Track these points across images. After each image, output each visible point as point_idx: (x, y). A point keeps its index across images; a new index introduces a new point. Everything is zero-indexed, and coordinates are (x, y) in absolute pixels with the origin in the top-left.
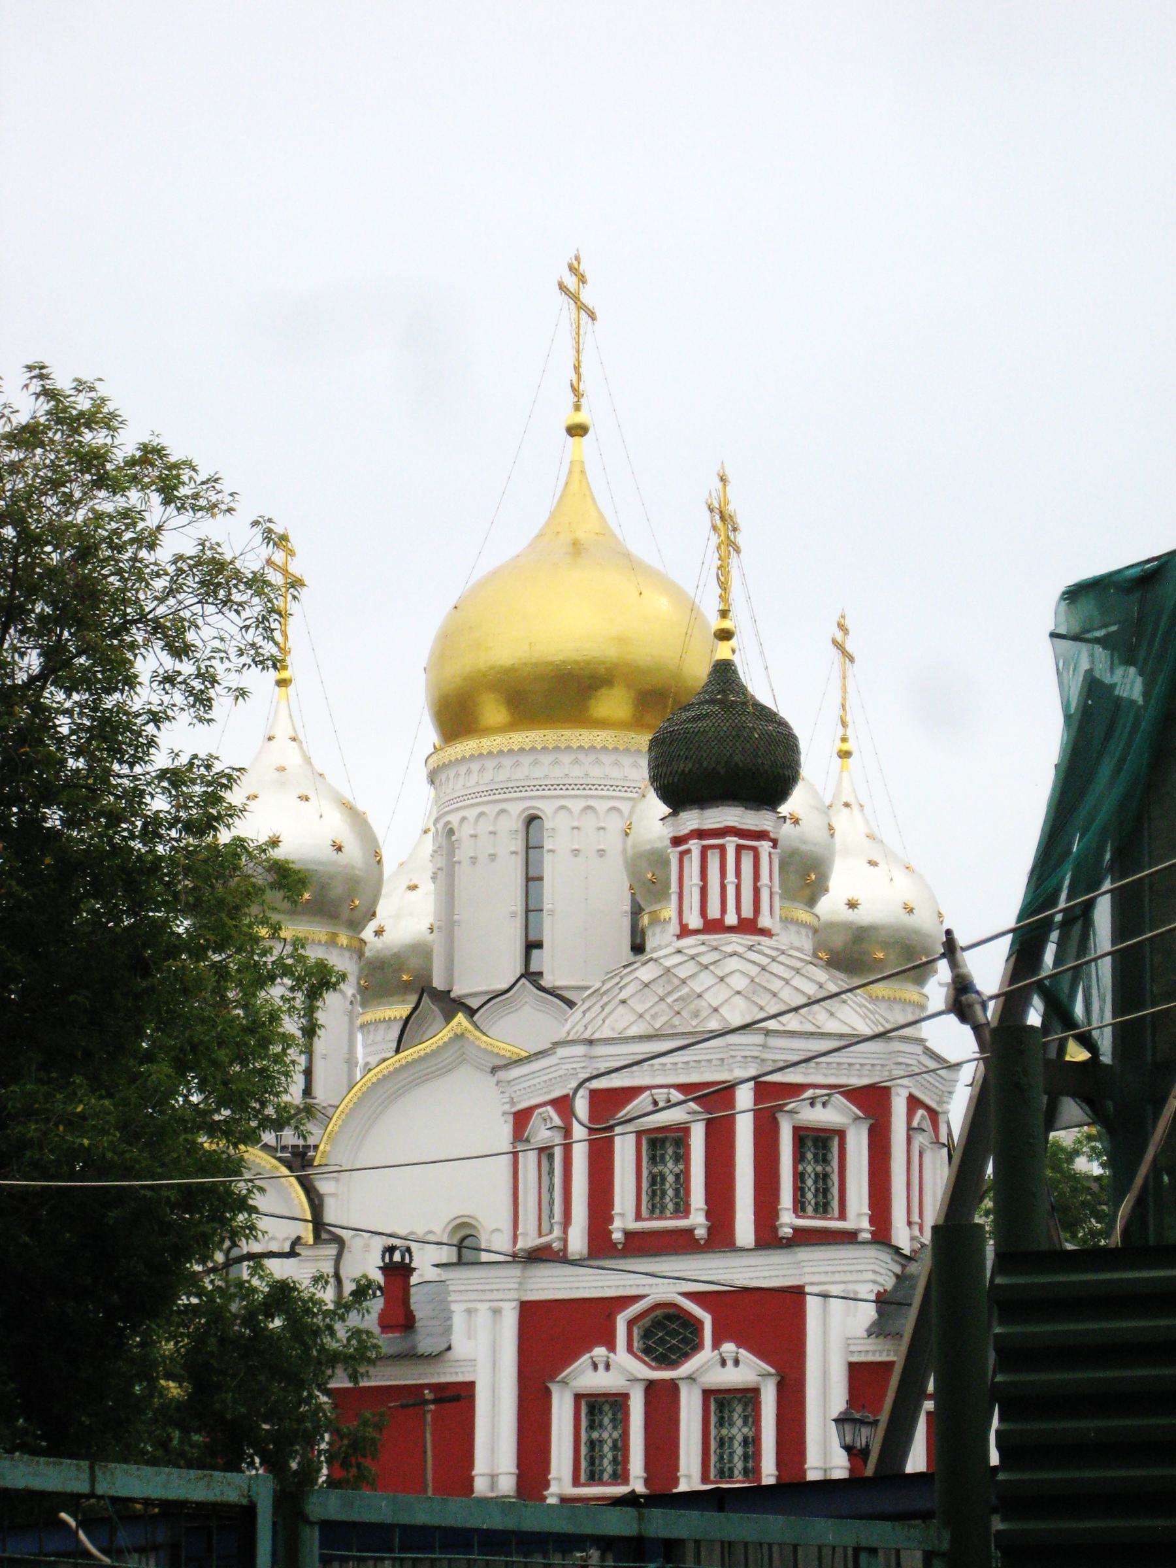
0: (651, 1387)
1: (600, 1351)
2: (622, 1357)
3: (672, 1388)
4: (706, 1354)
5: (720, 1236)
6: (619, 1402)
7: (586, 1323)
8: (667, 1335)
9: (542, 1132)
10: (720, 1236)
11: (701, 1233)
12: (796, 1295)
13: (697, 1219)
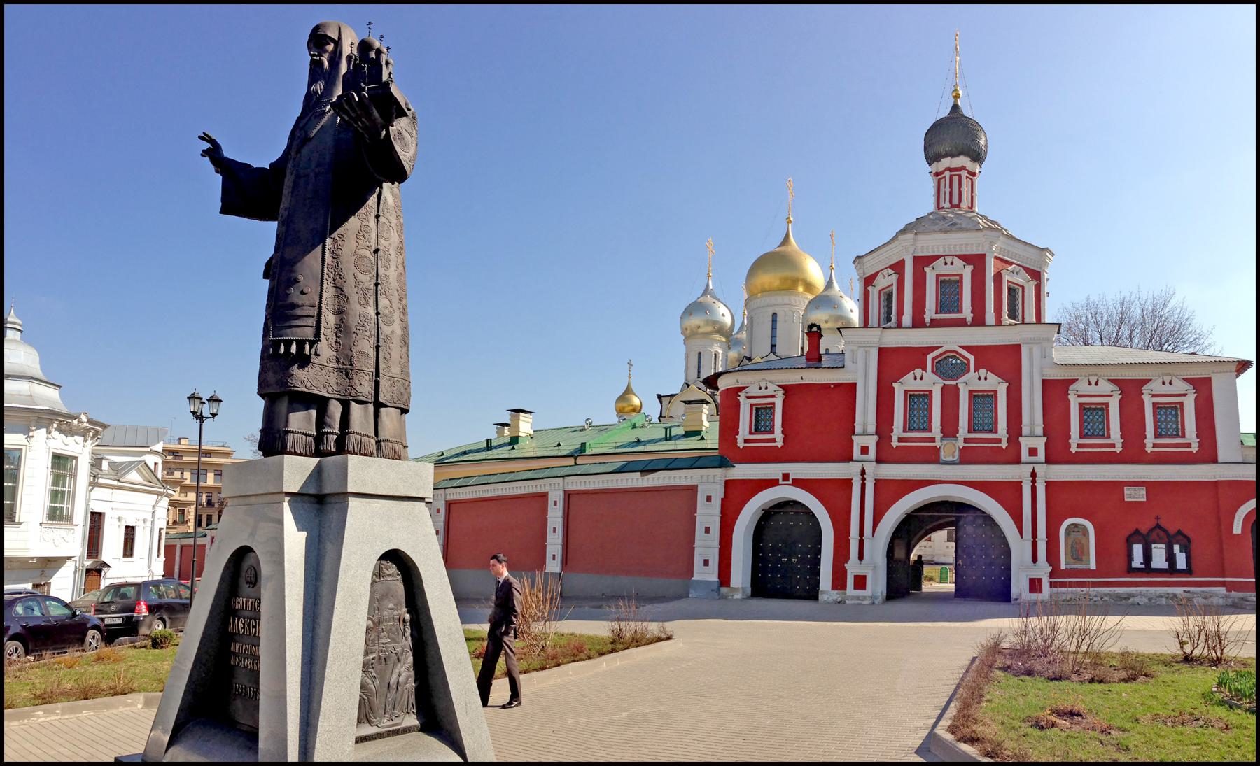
0: (944, 388)
1: (918, 372)
2: (929, 376)
3: (956, 388)
4: (972, 374)
5: (979, 321)
6: (928, 395)
7: (915, 357)
8: (948, 367)
9: (883, 282)
10: (979, 321)
11: (969, 319)
12: (1016, 349)
13: (967, 313)
